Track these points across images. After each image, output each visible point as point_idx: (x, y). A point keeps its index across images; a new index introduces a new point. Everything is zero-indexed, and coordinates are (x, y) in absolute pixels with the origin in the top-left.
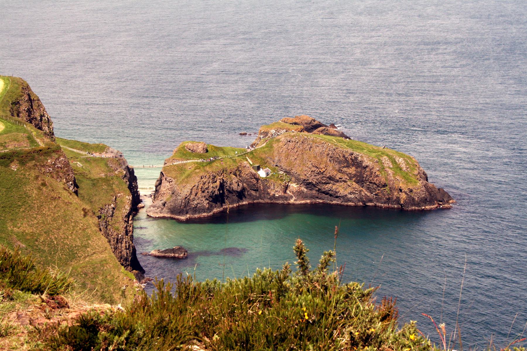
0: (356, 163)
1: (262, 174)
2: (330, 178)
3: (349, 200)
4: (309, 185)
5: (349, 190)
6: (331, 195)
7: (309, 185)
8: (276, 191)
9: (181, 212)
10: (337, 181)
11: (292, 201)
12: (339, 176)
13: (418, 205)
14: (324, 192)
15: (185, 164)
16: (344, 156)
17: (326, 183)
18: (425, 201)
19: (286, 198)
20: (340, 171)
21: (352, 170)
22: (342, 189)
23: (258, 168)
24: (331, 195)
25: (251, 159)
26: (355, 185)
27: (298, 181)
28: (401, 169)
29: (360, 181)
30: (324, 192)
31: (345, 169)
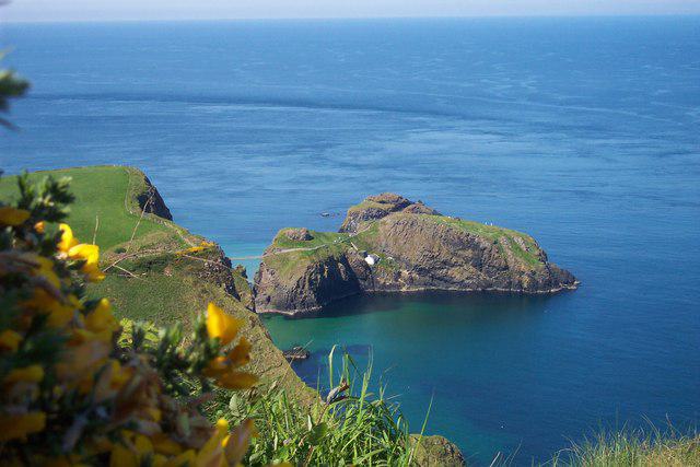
0: (470, 244)
1: (370, 260)
2: (445, 263)
3: (465, 286)
4: (421, 271)
5: (466, 275)
6: (446, 281)
7: (421, 271)
8: (385, 279)
9: (288, 307)
10: (453, 266)
11: (404, 289)
12: (454, 260)
13: (544, 288)
14: (439, 278)
15: (288, 253)
16: (459, 238)
17: (440, 268)
18: (548, 284)
19: (399, 286)
20: (454, 254)
21: (469, 253)
22: (456, 274)
23: (366, 256)
24: (446, 281)
25: (356, 244)
26: (472, 269)
27: (408, 266)
28: (521, 250)
29: (479, 265)
30: (439, 278)
31: (460, 252)
